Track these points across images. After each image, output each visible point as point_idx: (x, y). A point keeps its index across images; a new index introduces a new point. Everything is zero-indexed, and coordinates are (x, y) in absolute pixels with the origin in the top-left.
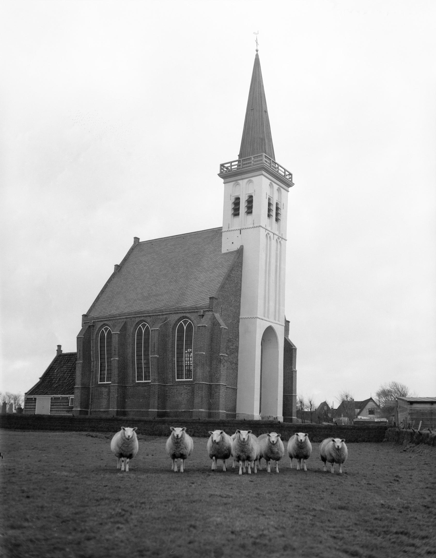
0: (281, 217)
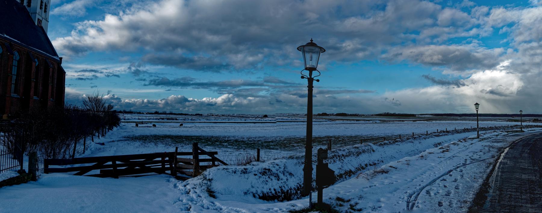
0: (47, 10)
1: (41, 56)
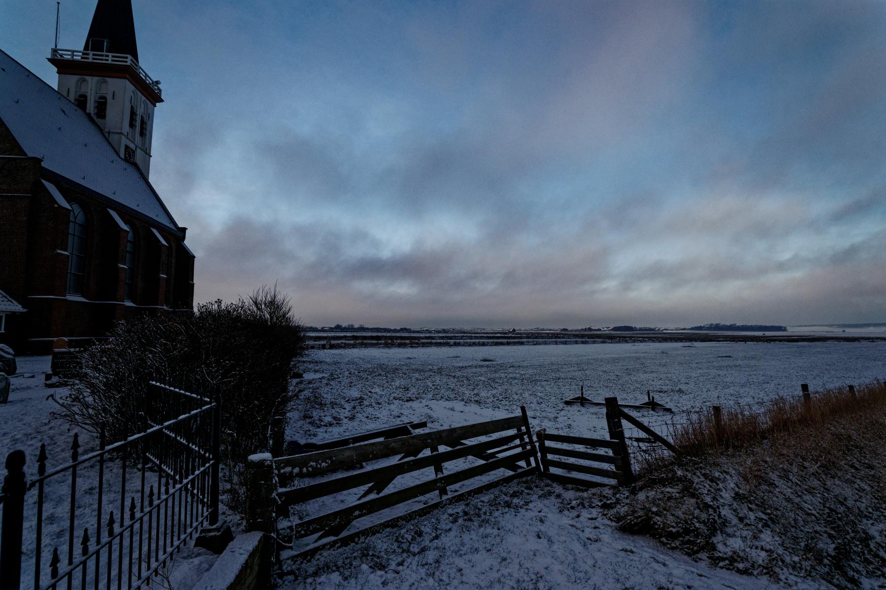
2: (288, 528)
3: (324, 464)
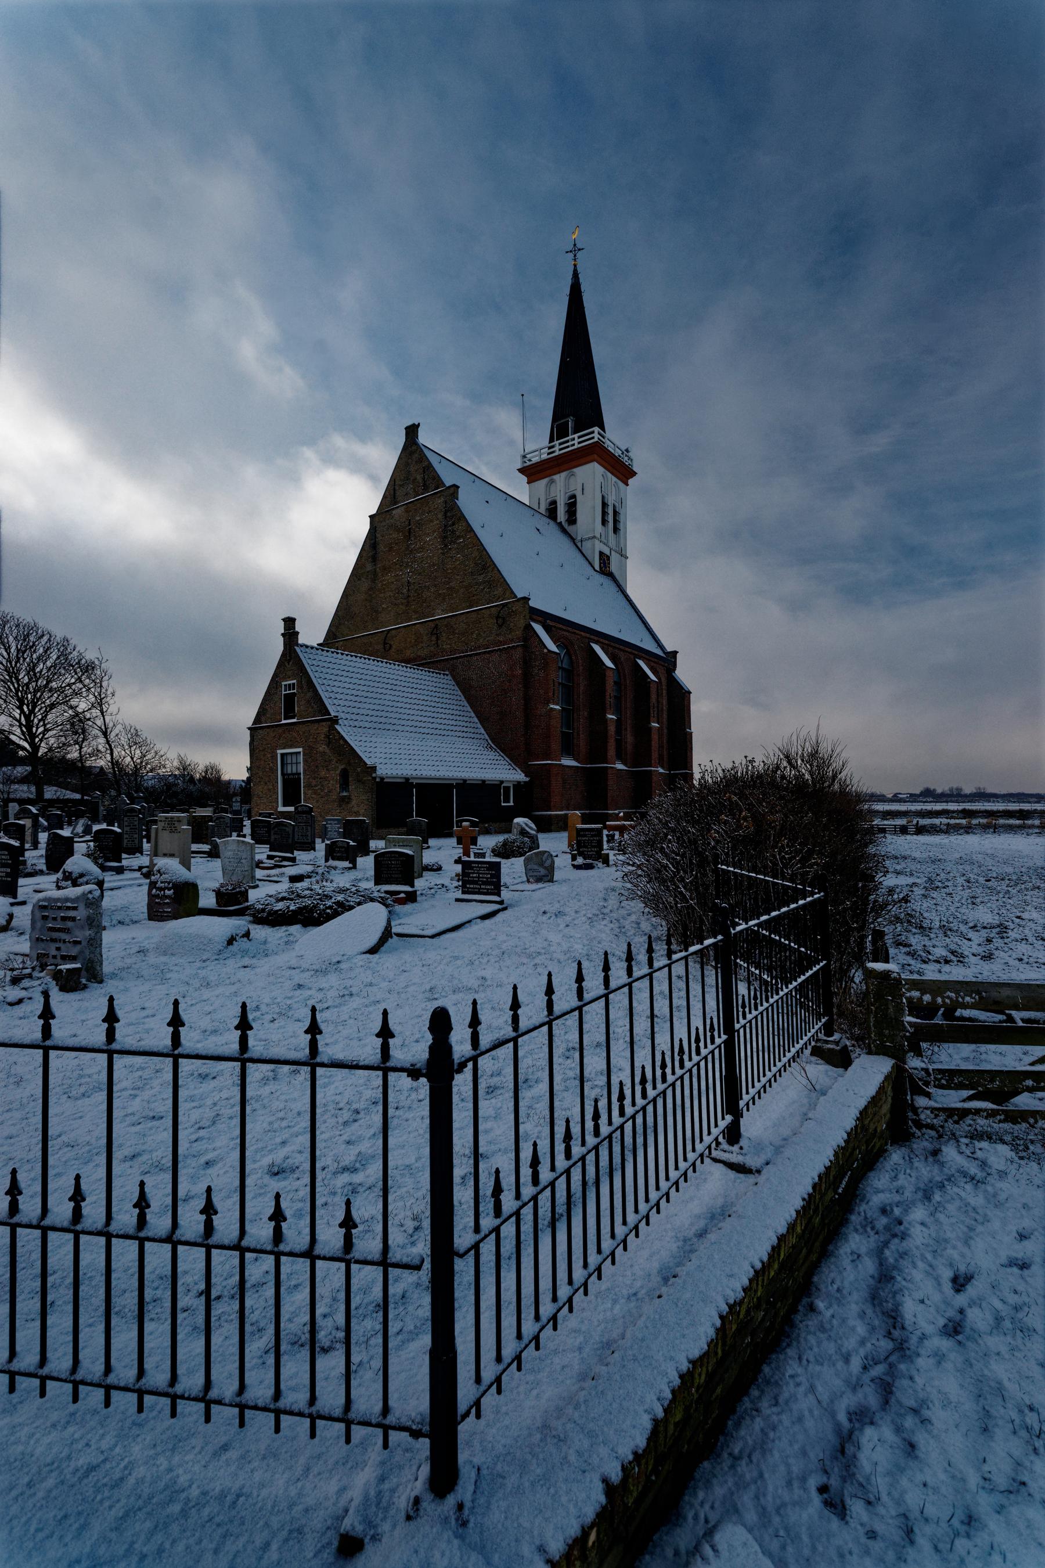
0: (621, 526)
1: (624, 651)
2: (922, 1069)
3: (968, 999)
